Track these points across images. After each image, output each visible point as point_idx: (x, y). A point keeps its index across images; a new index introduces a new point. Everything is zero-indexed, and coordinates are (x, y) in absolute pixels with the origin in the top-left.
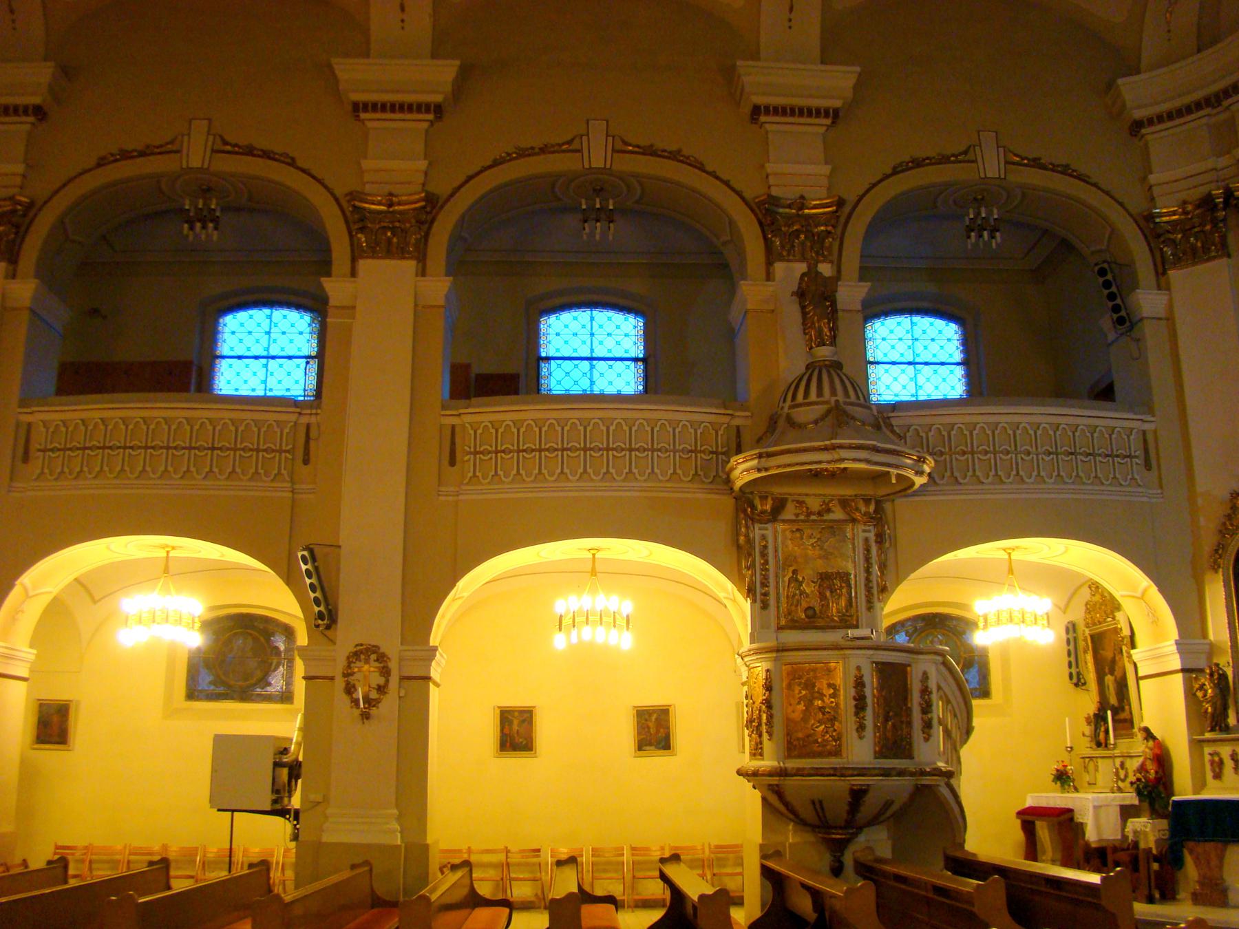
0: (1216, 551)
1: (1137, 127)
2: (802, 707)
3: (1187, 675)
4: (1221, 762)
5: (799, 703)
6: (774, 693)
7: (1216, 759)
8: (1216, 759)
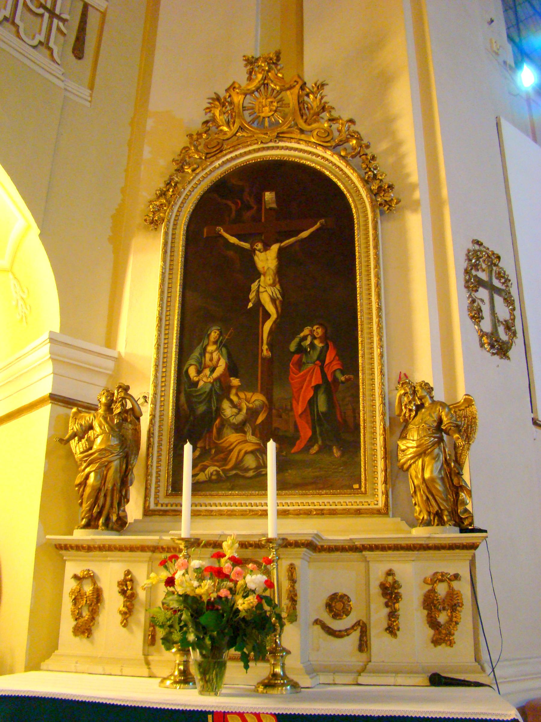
0: (163, 194)
3: (62, 410)
7: (88, 589)
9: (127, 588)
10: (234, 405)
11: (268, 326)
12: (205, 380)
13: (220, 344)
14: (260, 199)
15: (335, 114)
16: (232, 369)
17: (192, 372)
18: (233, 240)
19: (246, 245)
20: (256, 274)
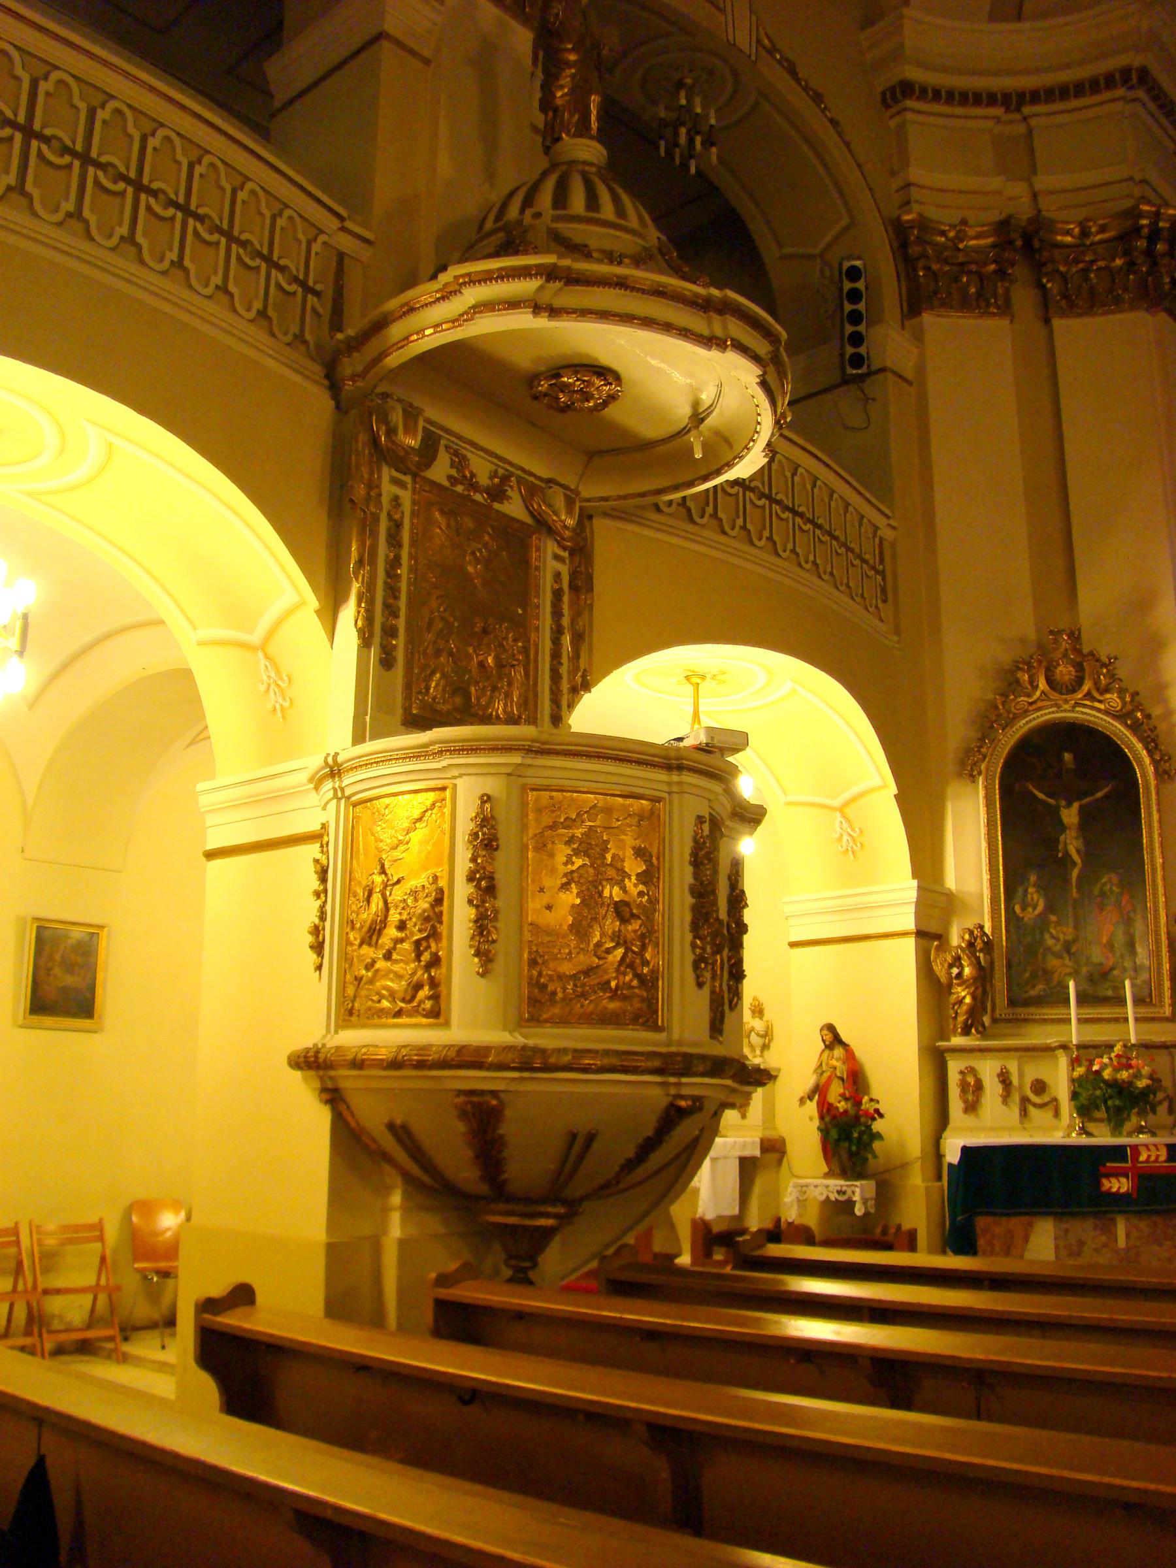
1: (906, 89)
2: (572, 898)
3: (923, 942)
4: (979, 1086)
5: (565, 887)
6: (500, 856)
8: (971, 1080)
9: (1004, 1078)
10: (1053, 937)
11: (1075, 873)
12: (1029, 915)
13: (1040, 887)
14: (1060, 760)
15: (1123, 685)
16: (1050, 908)
17: (1017, 908)
18: (1041, 796)
19: (1052, 801)
20: (1062, 828)
